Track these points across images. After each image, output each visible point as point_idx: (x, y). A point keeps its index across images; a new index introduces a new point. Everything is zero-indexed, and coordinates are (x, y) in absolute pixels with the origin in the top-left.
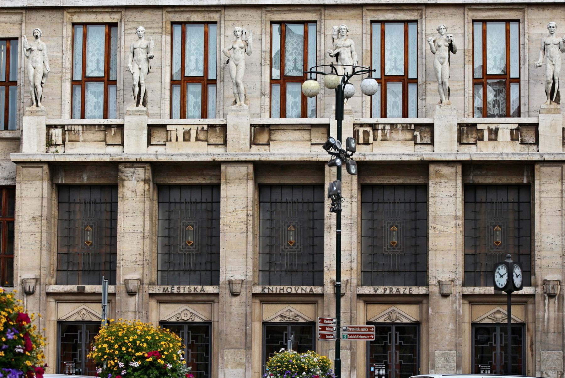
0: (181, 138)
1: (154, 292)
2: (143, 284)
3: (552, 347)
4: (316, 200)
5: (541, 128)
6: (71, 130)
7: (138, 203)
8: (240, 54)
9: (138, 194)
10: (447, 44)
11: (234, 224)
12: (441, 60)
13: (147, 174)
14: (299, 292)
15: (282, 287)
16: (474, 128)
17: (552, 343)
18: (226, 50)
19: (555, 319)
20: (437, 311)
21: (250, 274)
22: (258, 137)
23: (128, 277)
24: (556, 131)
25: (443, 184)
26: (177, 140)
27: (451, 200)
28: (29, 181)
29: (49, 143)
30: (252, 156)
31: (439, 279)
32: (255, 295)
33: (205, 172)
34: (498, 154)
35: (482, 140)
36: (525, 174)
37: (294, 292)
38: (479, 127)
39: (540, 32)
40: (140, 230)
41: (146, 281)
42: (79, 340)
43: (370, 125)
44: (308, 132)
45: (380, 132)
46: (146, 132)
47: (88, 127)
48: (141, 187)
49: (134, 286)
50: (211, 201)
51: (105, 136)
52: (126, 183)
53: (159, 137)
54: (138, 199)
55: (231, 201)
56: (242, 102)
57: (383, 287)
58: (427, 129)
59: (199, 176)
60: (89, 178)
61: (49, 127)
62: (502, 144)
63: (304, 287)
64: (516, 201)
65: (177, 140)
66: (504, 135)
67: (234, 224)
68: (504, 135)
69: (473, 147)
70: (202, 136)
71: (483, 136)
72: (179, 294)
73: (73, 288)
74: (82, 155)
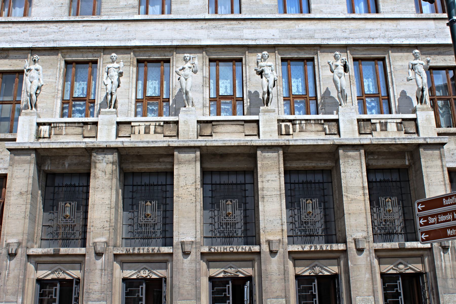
0: (142, 132)
1: (118, 253)
2: (109, 246)
3: (452, 291)
4: (246, 182)
5: (419, 121)
6: (57, 127)
7: (107, 181)
8: (188, 71)
9: (107, 173)
10: (342, 64)
11: (185, 196)
12: (340, 75)
13: (114, 158)
14: (240, 250)
15: (225, 247)
16: (369, 123)
17: (451, 287)
18: (178, 70)
19: (450, 267)
20: (355, 263)
21: (199, 236)
22: (203, 130)
23: (96, 240)
24: (430, 123)
25: (351, 163)
26: (139, 133)
27: (358, 174)
28: (19, 164)
29: (38, 137)
30: (199, 142)
31: (354, 237)
32: (202, 254)
33: (161, 160)
34: (392, 139)
35: (376, 130)
36: (407, 158)
37: (235, 250)
38: (373, 121)
39: (401, 64)
40: (108, 202)
41: (111, 243)
42: (54, 295)
43: (290, 121)
44: (242, 126)
45: (298, 126)
46: (115, 126)
47: (70, 125)
48: (110, 168)
49: (101, 248)
50: (165, 183)
51: (83, 131)
52: (98, 165)
53: (125, 130)
54: (107, 177)
55: (182, 178)
56: (190, 106)
57: (309, 245)
58: (334, 123)
59: (156, 162)
60: (69, 165)
61: (39, 124)
62: (391, 134)
63: (244, 247)
64: (398, 180)
65: (139, 133)
66: (392, 127)
67: (185, 196)
68: (392, 127)
69: (370, 136)
70: (159, 129)
71: (376, 128)
72: (139, 255)
73: (51, 250)
74: (63, 142)
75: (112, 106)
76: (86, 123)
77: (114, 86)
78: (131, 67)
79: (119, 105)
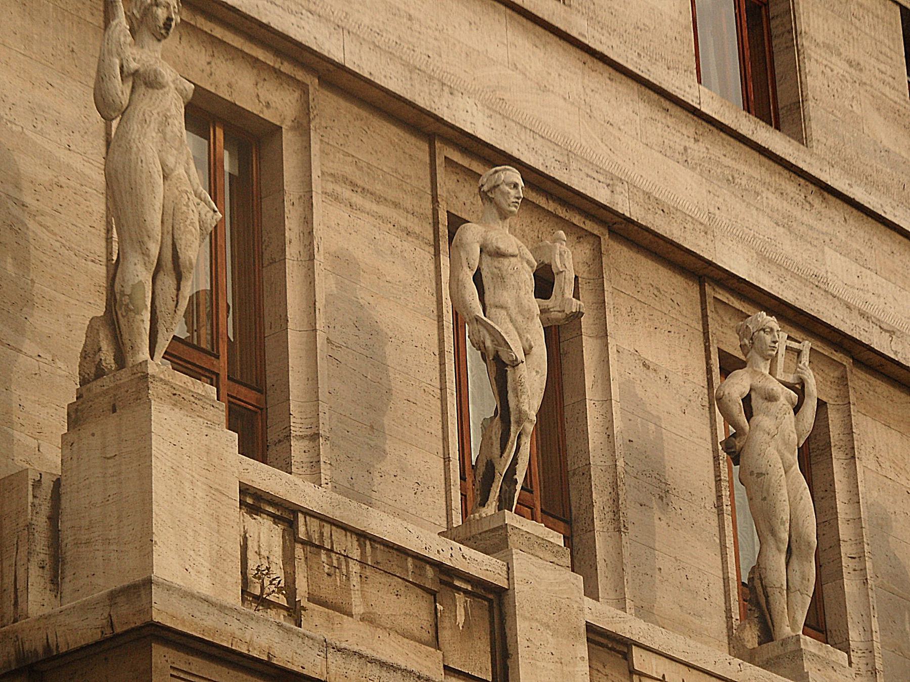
46: (583, 649)
76: (447, 574)
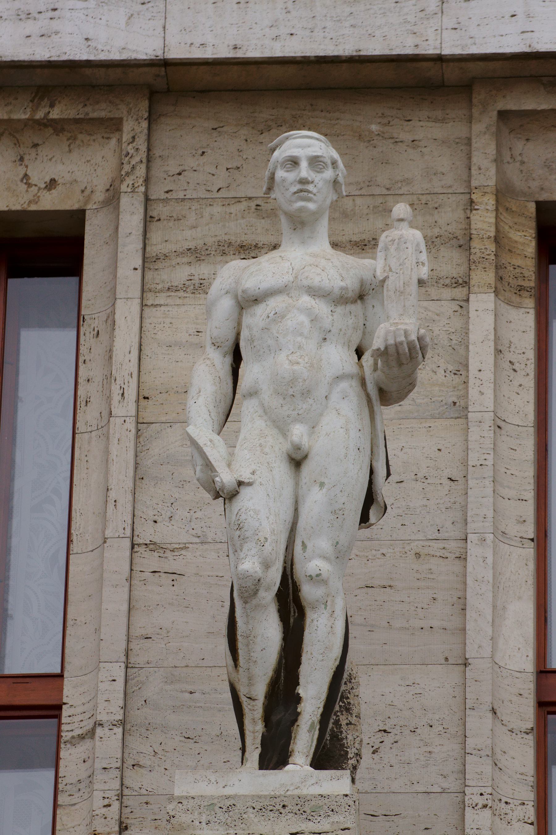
75: (304, 741)
77: (315, 502)
78: (483, 304)
79: (361, 734)
